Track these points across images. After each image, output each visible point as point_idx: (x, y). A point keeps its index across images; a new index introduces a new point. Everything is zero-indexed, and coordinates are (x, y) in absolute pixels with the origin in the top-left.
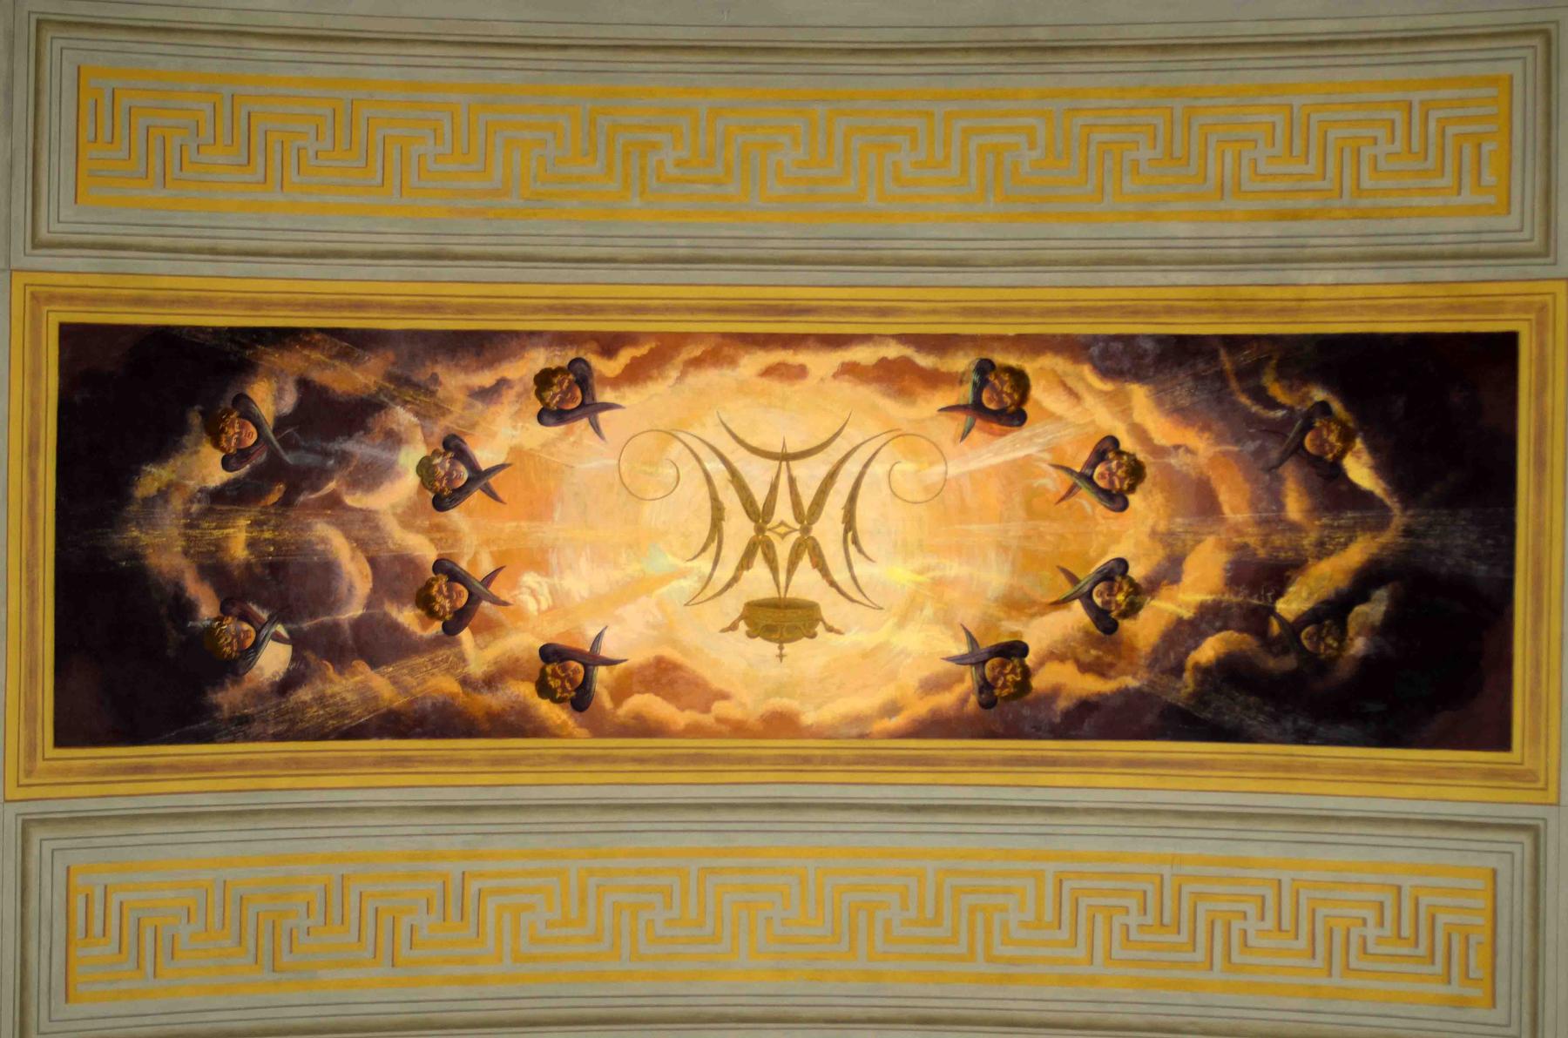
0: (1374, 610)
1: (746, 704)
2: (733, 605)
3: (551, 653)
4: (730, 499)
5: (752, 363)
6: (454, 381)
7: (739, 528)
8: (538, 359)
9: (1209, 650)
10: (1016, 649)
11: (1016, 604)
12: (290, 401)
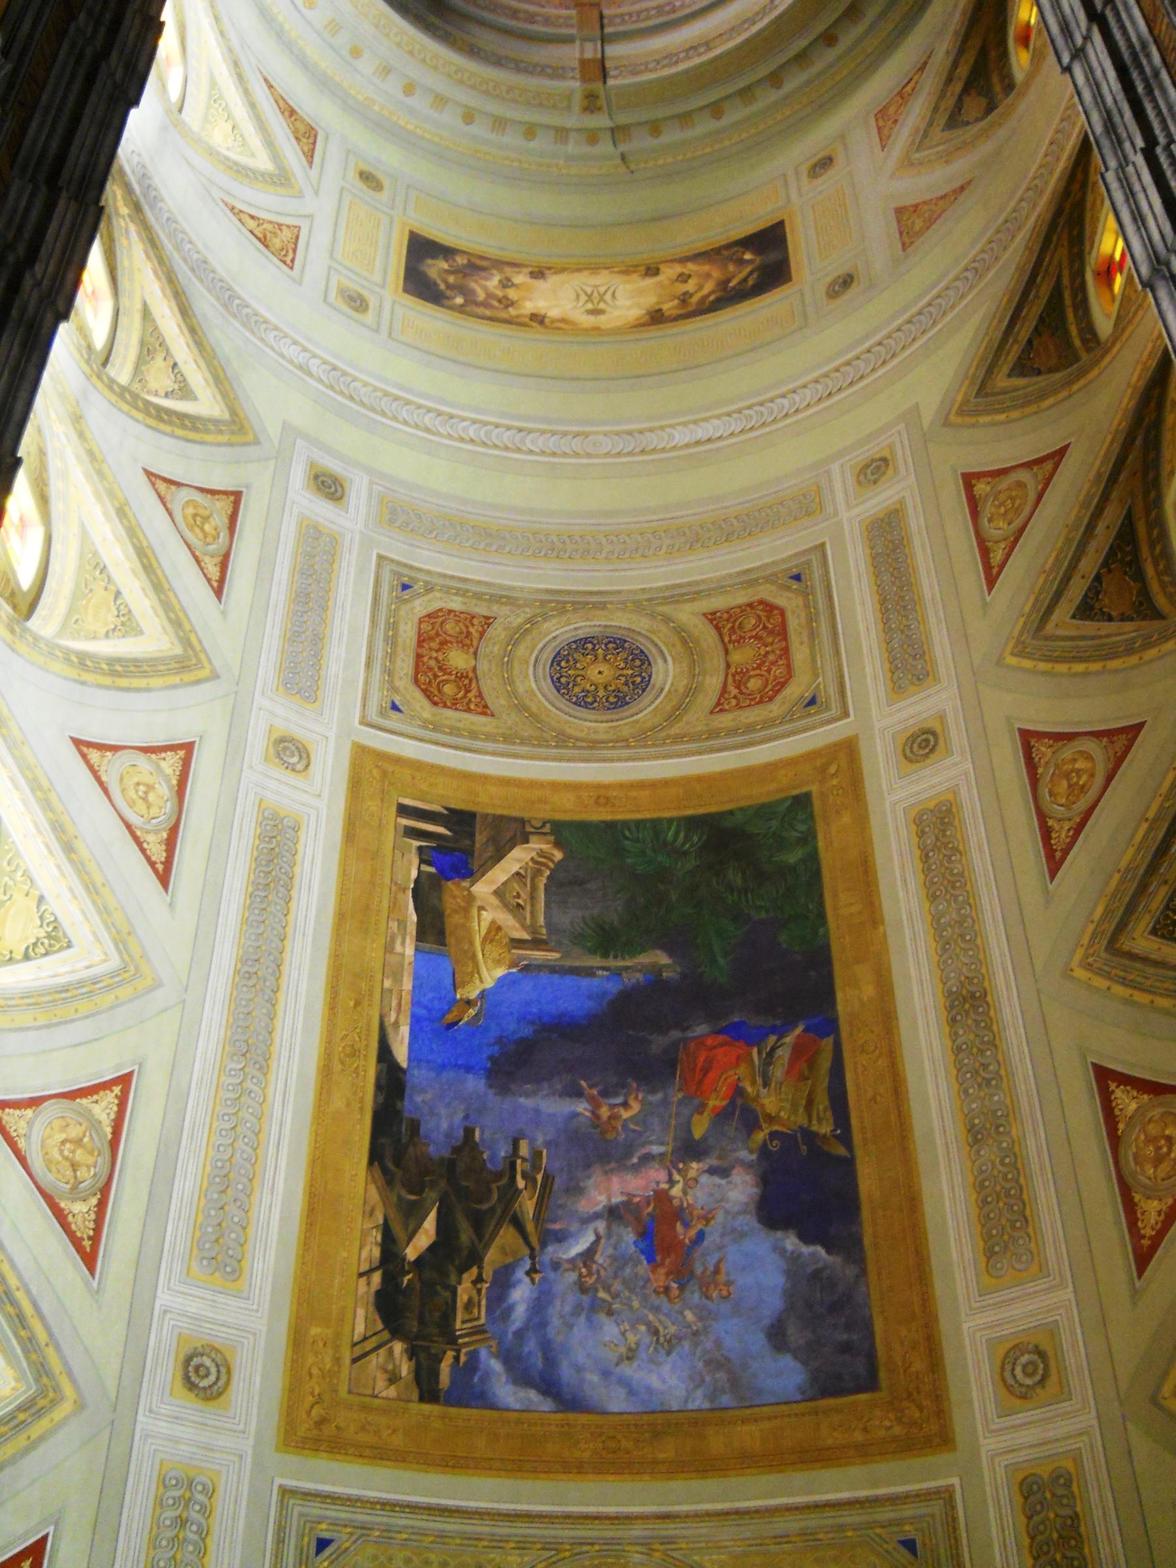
0: (755, 275)
1: (585, 325)
2: (583, 310)
3: (532, 315)
4: (581, 293)
5: (586, 273)
6: (508, 271)
7: (583, 298)
8: (530, 269)
9: (712, 298)
10: (660, 310)
11: (658, 303)
12: (465, 262)
